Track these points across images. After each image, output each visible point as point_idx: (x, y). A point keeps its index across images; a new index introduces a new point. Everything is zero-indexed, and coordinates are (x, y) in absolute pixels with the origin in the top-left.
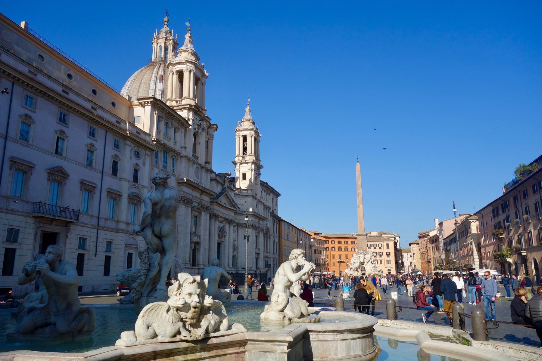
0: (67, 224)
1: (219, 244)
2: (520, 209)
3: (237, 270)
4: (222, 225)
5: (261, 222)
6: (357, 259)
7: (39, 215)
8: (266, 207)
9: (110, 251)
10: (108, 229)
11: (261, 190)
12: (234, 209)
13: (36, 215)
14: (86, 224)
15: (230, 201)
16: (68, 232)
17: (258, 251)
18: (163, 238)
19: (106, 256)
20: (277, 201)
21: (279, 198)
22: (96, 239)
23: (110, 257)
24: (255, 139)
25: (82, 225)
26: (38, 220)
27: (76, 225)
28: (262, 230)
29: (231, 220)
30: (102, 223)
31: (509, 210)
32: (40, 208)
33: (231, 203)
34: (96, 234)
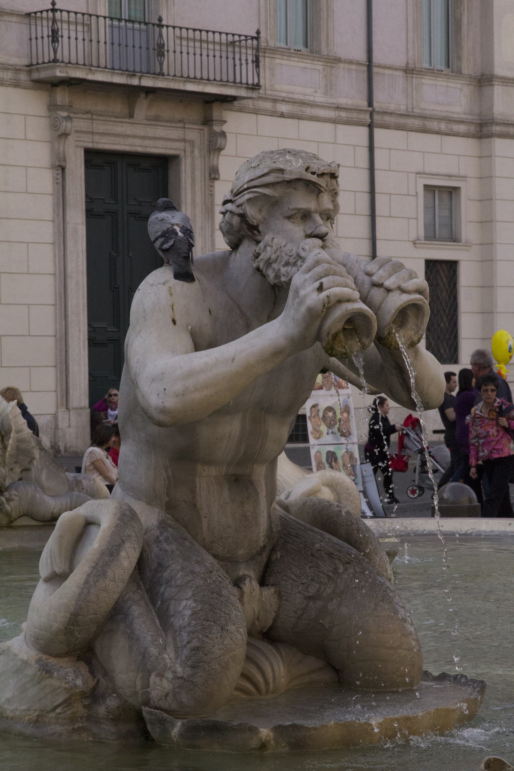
0: (208, 106)
7: (59, 73)
9: (453, 238)
10: (423, 123)
13: (44, 75)
14: (303, 103)
16: (214, 146)
19: (431, 266)
22: (365, 175)
23: (452, 266)
25: (283, 108)
26: (61, 96)
27: (256, 112)
30: (390, 95)
32: (55, 36)
34: (364, 153)
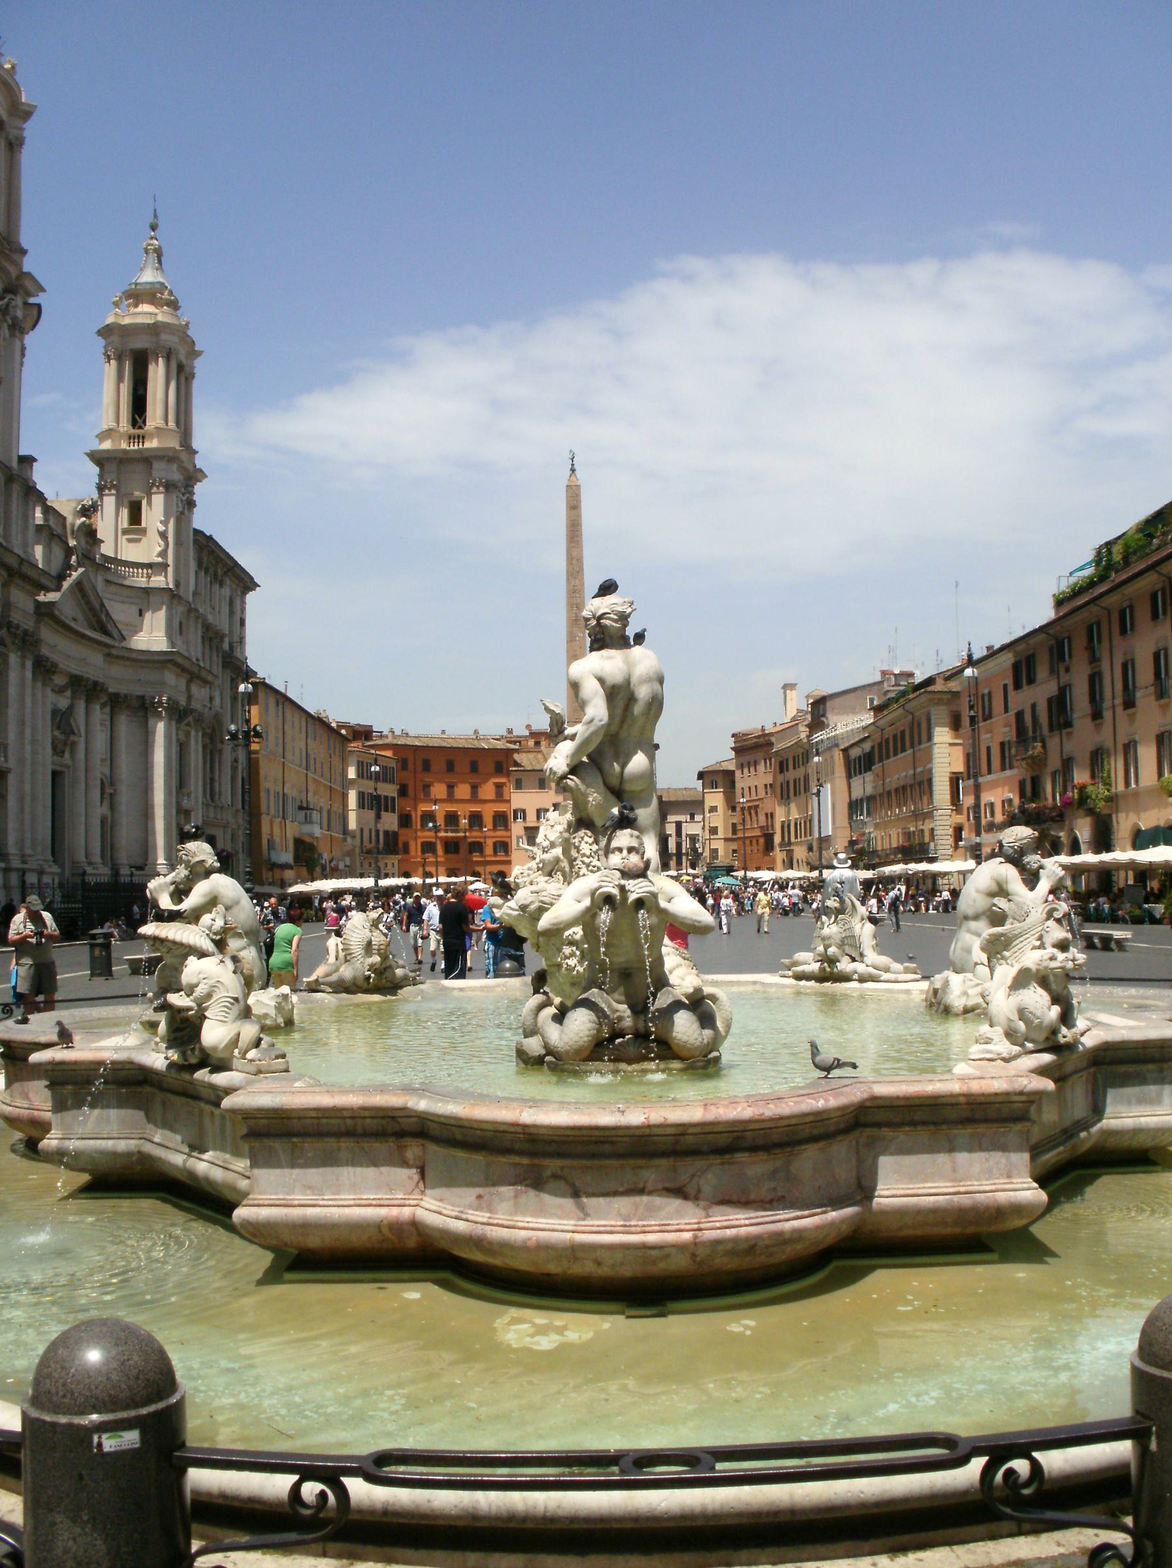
1: (55, 775)
2: (1105, 666)
3: (116, 874)
4: (63, 703)
5: (195, 689)
6: (560, 828)
8: (212, 636)
11: (193, 566)
12: (107, 640)
15: (92, 609)
17: (185, 803)
20: (243, 610)
21: (250, 597)
24: (181, 368)
28: (199, 720)
29: (96, 683)
31: (1067, 670)
33: (96, 615)
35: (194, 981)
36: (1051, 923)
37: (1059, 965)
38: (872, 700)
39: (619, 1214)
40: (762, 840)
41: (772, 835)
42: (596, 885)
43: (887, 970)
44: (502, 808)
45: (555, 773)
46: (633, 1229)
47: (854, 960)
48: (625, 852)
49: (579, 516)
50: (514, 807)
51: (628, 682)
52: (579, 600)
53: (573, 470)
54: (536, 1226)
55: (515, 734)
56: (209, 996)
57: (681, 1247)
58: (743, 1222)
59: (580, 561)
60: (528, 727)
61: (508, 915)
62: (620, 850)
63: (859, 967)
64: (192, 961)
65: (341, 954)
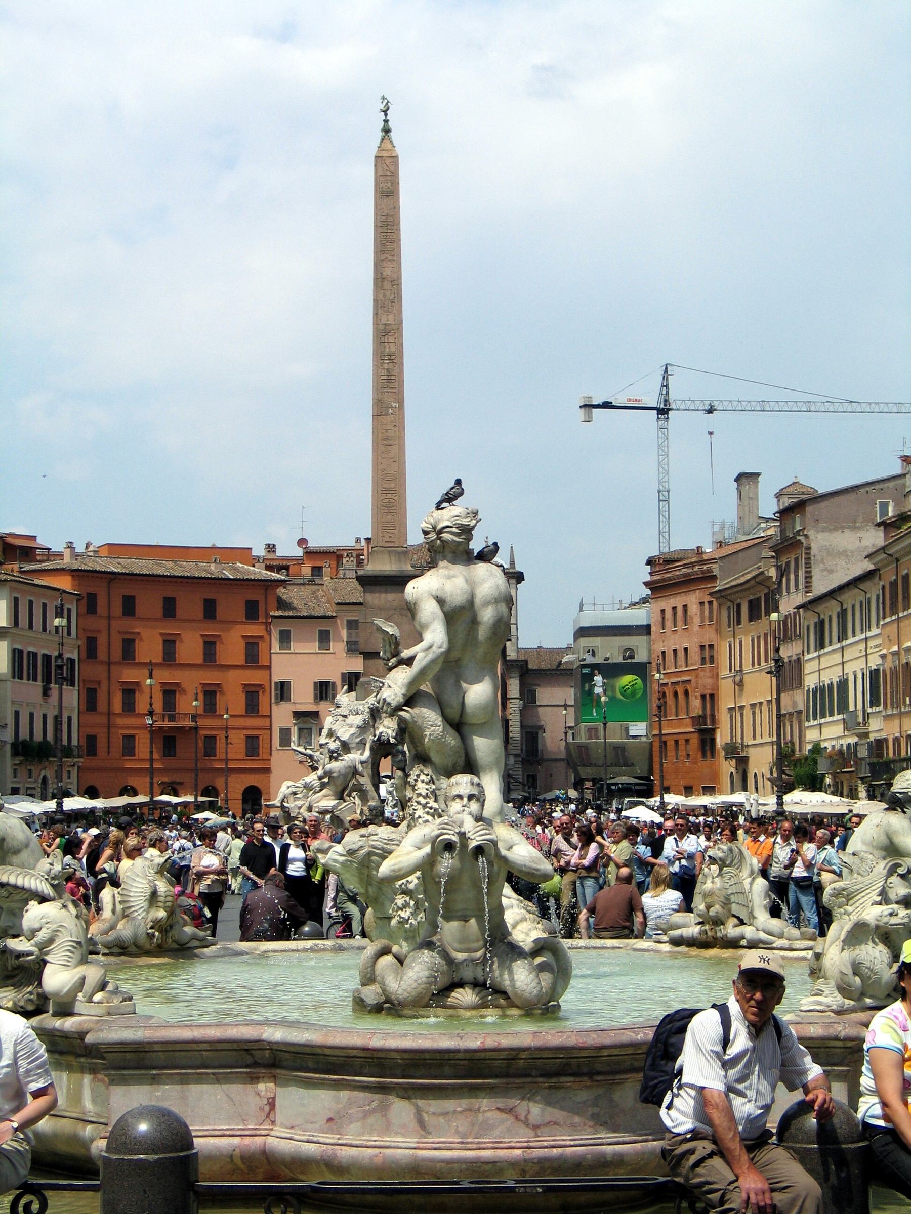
6: (358, 720)
18: (465, 730)
35: (37, 926)
36: (894, 879)
37: (900, 921)
38: (884, 506)
39: (457, 1132)
40: (695, 740)
41: (713, 731)
42: (437, 832)
43: (781, 936)
44: (254, 677)
45: (389, 704)
46: (469, 1146)
47: (742, 922)
48: (465, 799)
49: (396, 208)
50: (277, 678)
51: (471, 603)
52: (393, 349)
53: (387, 131)
54: (382, 1144)
55: (280, 552)
56: (51, 941)
57: (513, 1164)
58: (568, 1143)
59: (396, 283)
60: (302, 542)
61: (335, 861)
62: (460, 797)
63: (748, 931)
64: (33, 904)
65: (119, 907)
